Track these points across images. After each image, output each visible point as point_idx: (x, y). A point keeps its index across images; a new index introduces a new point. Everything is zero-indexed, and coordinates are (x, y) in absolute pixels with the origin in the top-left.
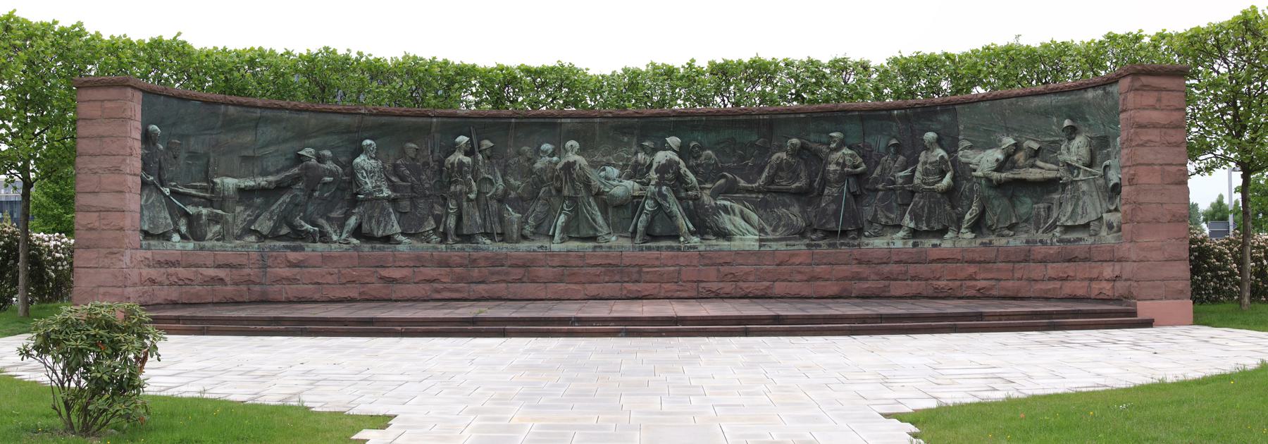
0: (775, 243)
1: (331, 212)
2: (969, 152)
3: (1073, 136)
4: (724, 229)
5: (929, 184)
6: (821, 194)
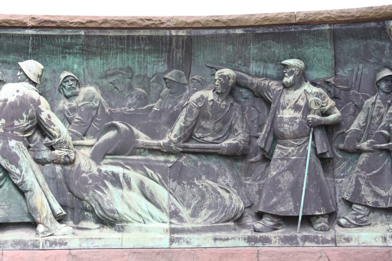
0: (196, 236)
4: (113, 211)
6: (267, 159)
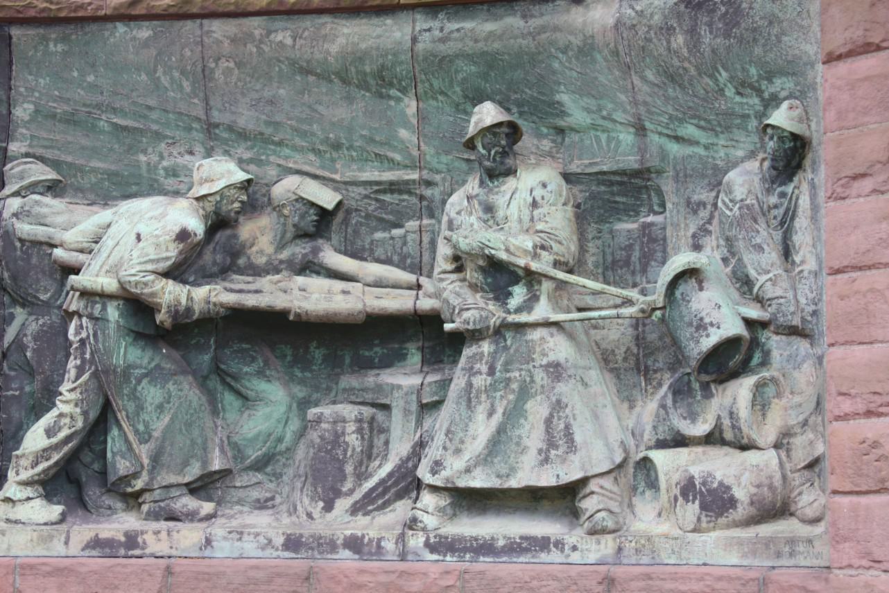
2: (50, 204)
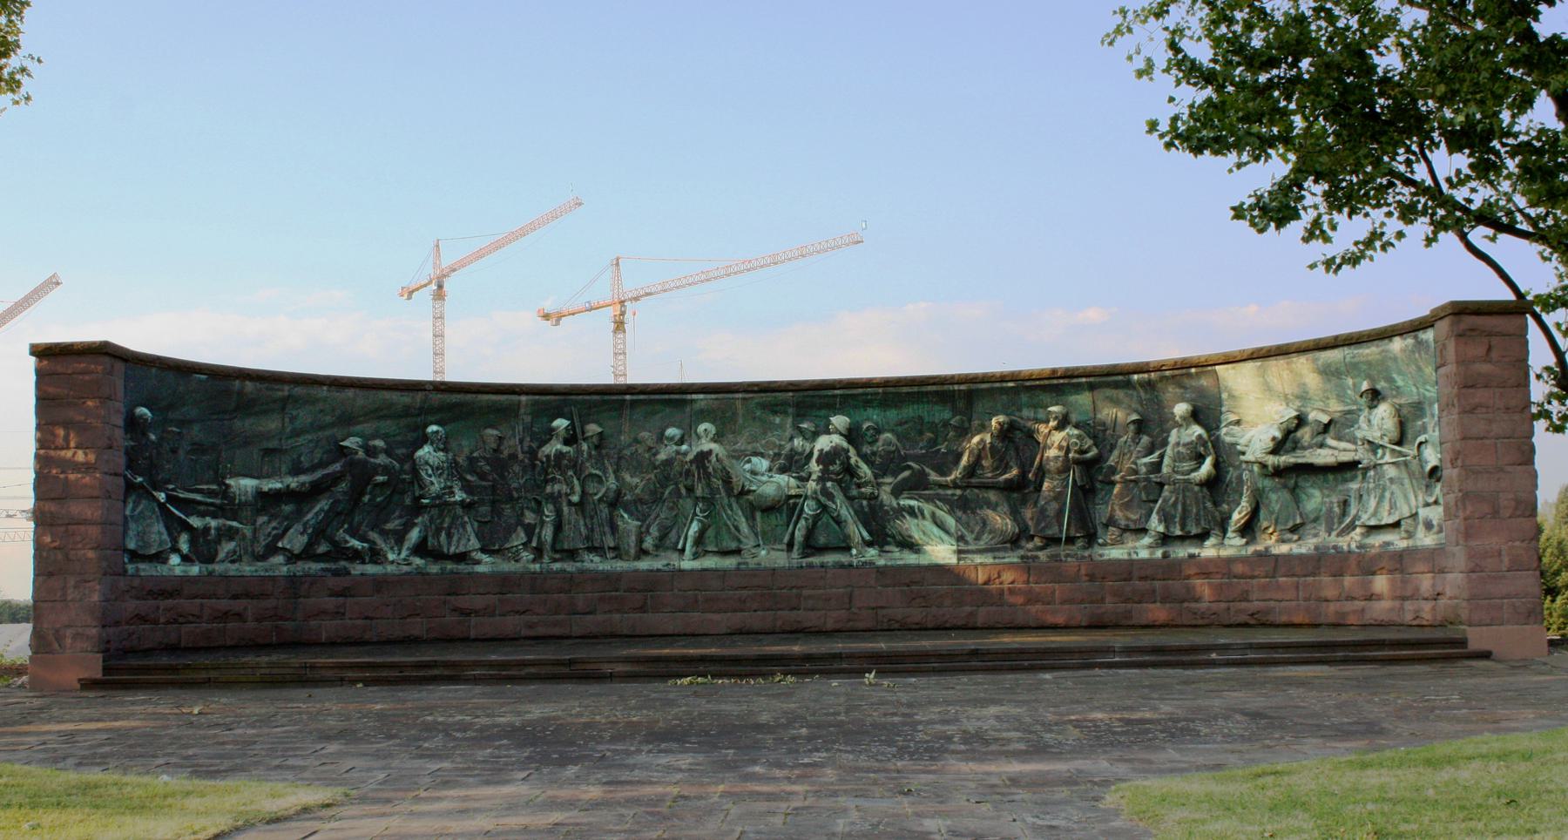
1: (387, 521)
3: (1375, 403)
4: (910, 537)
5: (1183, 474)
6: (1039, 488)
